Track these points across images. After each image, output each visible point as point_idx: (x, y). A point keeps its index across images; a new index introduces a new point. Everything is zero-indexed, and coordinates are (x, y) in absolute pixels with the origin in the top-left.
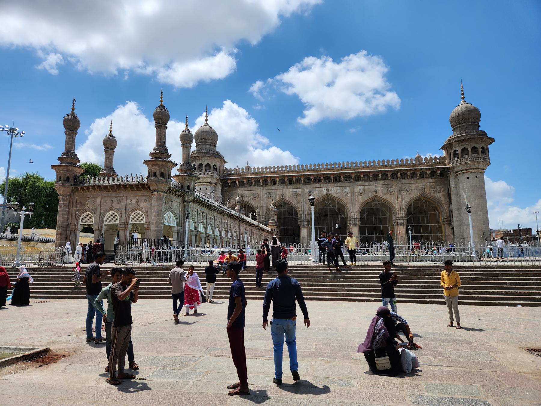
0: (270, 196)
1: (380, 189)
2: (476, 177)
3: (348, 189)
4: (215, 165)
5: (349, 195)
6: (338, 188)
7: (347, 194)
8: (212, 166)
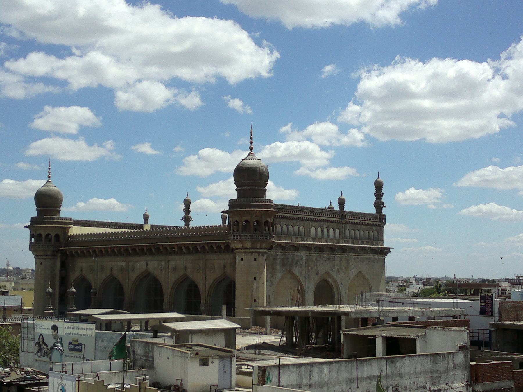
0: (103, 268)
1: (189, 265)
2: (242, 259)
3: (163, 263)
4: (49, 235)
5: (164, 272)
6: (156, 263)
7: (162, 270)
8: (43, 236)
